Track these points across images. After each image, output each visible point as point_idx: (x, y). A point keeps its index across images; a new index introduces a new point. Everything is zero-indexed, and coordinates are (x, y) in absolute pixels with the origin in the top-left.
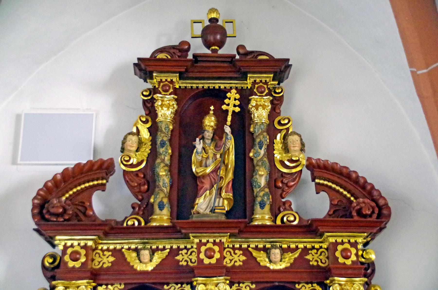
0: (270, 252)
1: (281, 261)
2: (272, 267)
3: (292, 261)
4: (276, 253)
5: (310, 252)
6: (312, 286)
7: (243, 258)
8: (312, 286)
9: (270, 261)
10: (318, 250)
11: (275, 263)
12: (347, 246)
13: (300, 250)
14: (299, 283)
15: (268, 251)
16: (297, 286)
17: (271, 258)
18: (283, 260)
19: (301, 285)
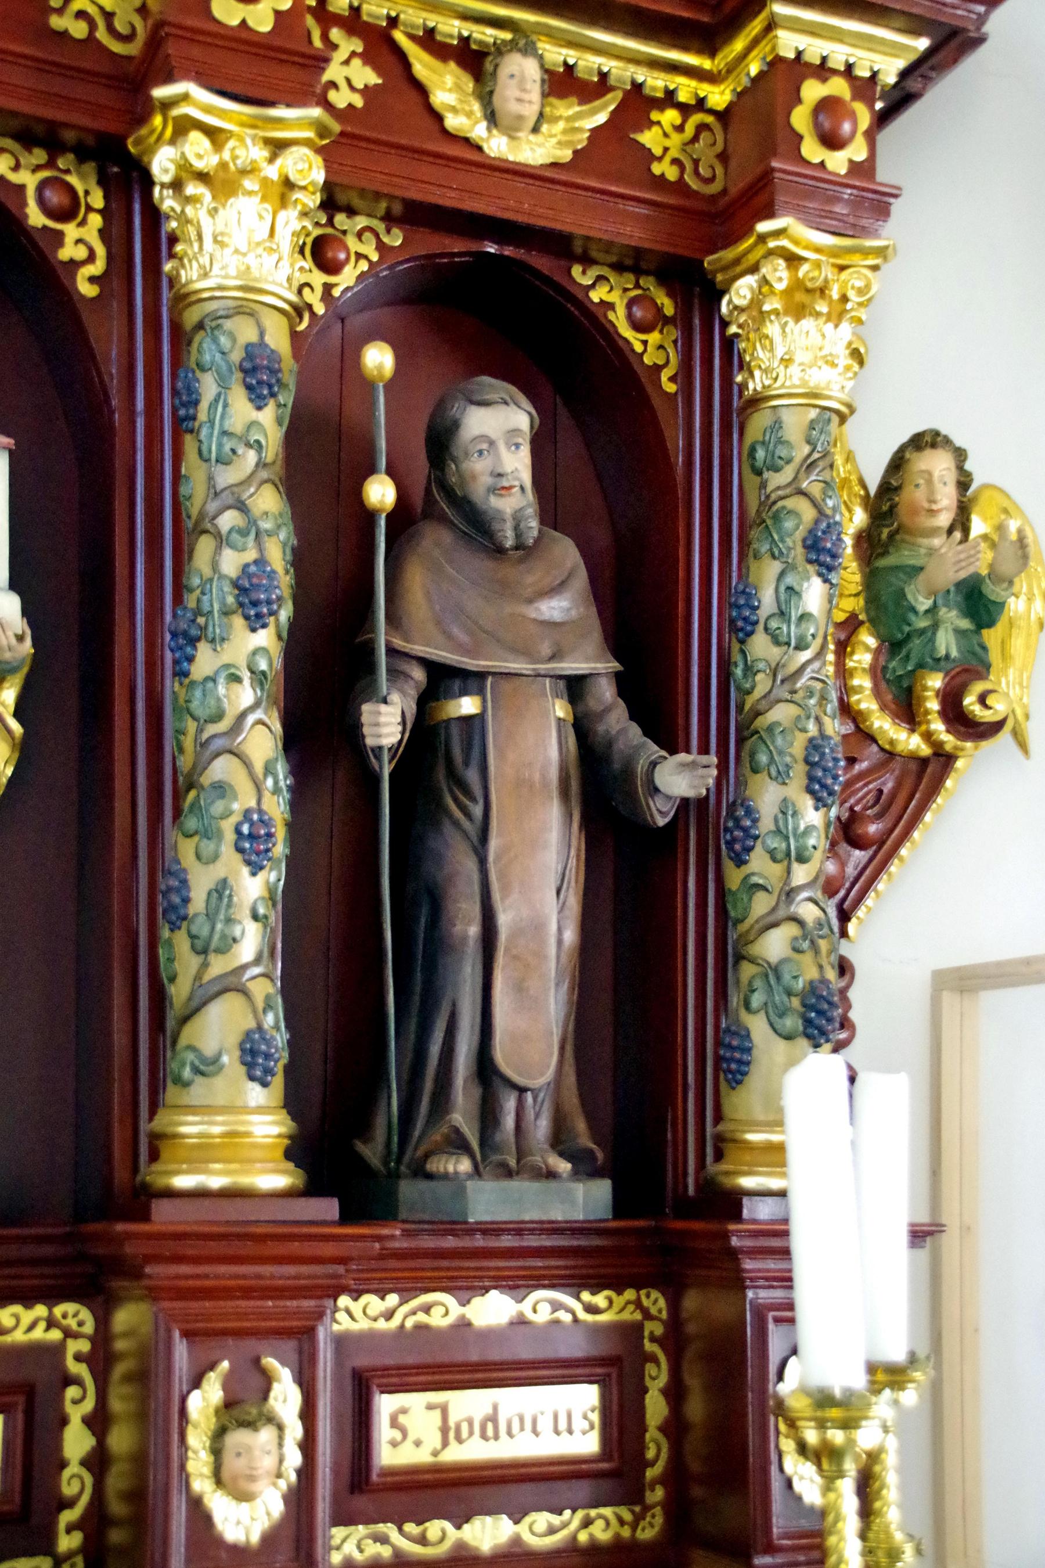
0: (496, 66)
1: (535, 130)
2: (497, 146)
3: (582, 140)
4: (521, 78)
5: (655, 116)
6: (637, 286)
7: (366, 76)
8: (637, 286)
9: (492, 118)
10: (685, 110)
11: (511, 132)
12: (838, 87)
13: (619, 95)
14: (587, 261)
15: (488, 66)
16: (576, 271)
17: (496, 99)
18: (545, 128)
19: (594, 272)
